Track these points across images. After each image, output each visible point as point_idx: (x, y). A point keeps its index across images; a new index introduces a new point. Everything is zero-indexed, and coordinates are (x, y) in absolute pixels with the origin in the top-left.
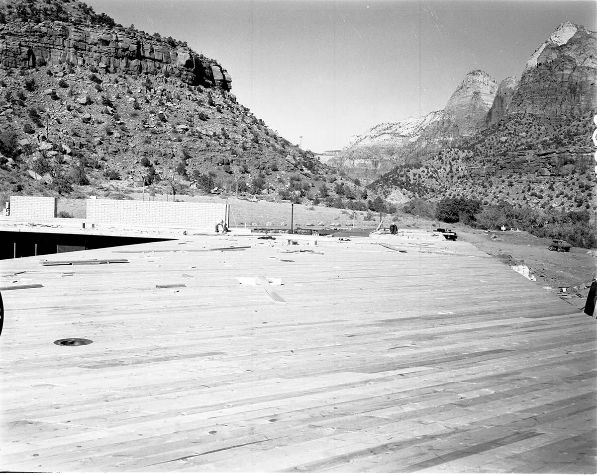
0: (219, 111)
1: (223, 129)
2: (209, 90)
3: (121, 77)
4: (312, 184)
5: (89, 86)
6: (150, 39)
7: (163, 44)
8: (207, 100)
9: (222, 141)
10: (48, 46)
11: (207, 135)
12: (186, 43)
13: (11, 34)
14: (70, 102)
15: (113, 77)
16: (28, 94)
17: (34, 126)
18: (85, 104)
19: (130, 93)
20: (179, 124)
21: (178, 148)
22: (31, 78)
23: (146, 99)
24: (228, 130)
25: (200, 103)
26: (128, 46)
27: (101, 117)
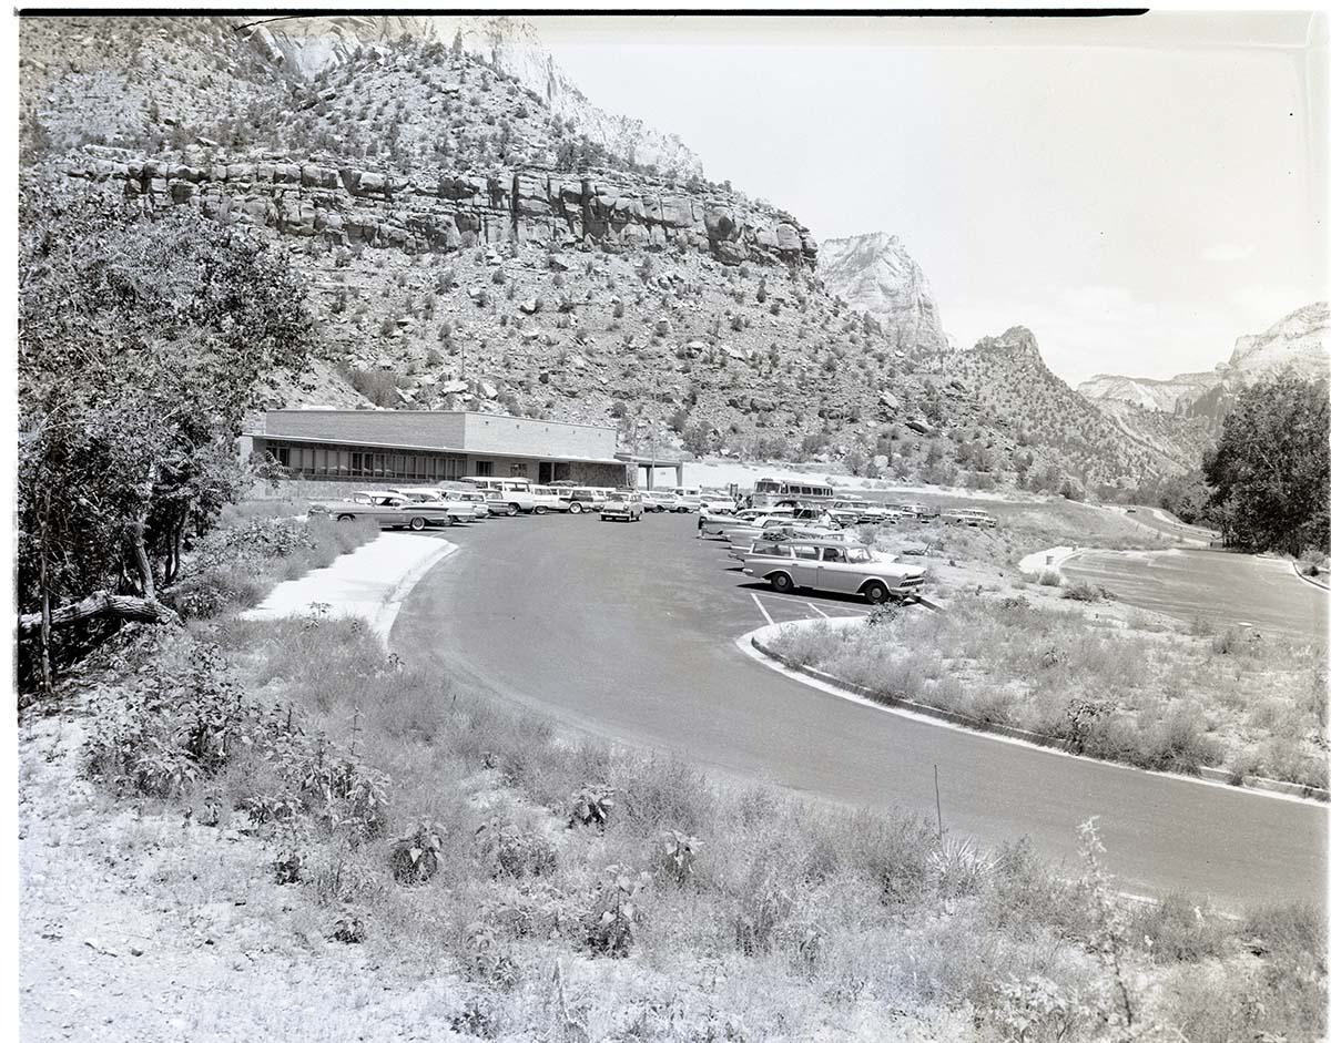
0: (775, 311)
1: (773, 347)
2: (765, 270)
5: (546, 277)
6: (656, 185)
7: (679, 190)
8: (756, 291)
9: (765, 369)
10: (483, 210)
11: (740, 359)
12: (727, 186)
13: (419, 193)
14: (508, 308)
15: (587, 258)
16: (440, 300)
17: (444, 353)
18: (529, 313)
19: (611, 287)
20: (690, 341)
22: (449, 269)
24: (784, 348)
25: (739, 298)
26: (614, 200)
27: (554, 334)
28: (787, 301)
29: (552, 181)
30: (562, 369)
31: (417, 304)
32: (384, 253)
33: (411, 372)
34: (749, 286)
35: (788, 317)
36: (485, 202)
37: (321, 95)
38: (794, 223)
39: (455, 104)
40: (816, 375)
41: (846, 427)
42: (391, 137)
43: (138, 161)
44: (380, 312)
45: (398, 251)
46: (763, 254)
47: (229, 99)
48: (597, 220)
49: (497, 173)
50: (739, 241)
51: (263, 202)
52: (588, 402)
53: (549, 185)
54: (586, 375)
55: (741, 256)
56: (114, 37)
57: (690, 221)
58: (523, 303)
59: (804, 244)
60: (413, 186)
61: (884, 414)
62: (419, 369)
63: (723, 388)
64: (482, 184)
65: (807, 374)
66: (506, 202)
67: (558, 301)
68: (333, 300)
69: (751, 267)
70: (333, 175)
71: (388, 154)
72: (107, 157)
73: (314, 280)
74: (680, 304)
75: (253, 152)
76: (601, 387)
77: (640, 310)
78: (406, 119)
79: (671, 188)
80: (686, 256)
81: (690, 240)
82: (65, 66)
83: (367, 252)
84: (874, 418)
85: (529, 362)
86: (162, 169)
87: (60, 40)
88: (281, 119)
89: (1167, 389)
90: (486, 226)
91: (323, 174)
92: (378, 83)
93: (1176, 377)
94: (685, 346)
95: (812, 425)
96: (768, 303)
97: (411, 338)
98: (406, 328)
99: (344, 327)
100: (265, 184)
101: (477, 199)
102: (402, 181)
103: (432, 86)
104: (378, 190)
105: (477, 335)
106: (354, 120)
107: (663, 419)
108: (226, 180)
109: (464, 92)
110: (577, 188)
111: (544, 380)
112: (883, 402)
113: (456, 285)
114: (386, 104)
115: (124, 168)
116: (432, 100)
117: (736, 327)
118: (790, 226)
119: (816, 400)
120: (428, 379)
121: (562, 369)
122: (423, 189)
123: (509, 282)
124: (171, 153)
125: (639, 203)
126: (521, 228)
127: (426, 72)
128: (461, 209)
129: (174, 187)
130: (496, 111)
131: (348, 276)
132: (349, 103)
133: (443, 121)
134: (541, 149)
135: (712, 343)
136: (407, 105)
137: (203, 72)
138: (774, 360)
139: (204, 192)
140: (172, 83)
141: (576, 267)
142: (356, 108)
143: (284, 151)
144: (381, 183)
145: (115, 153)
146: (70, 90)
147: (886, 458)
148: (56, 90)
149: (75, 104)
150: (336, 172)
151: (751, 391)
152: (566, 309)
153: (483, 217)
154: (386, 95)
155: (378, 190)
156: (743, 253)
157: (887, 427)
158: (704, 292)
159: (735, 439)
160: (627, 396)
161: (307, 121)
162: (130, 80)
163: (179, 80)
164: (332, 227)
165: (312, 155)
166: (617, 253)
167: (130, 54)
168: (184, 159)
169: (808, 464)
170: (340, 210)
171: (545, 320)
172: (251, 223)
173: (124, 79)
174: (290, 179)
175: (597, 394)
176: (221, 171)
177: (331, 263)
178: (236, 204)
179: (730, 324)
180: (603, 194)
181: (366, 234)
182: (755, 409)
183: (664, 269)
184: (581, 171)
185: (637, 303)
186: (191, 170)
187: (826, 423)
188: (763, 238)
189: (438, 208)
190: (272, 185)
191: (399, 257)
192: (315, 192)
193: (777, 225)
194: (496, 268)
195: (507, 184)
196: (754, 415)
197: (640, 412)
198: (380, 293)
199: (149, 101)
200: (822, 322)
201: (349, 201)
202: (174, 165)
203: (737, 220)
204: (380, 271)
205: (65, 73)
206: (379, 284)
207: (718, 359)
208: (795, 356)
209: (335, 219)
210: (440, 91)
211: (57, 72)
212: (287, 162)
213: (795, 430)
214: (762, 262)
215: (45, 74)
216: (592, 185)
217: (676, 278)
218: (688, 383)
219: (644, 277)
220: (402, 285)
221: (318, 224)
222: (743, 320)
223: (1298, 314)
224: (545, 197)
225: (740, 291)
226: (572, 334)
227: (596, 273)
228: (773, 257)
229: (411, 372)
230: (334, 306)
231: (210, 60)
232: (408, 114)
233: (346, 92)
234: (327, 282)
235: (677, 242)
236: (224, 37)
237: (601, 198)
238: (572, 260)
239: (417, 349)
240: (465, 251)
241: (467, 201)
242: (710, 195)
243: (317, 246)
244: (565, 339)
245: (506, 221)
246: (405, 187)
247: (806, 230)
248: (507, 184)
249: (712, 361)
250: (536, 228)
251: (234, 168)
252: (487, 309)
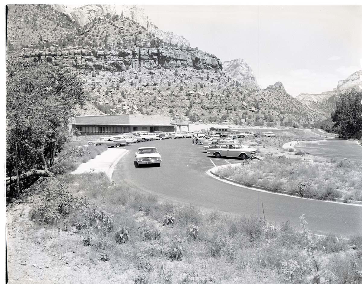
0: (212, 82)
1: (212, 91)
2: (209, 71)
3: (163, 70)
4: (254, 115)
5: (149, 76)
7: (184, 51)
9: (210, 98)
10: (131, 59)
12: (197, 49)
13: (113, 56)
14: (139, 85)
15: (160, 70)
17: (123, 99)
18: (145, 86)
19: (167, 78)
20: (189, 91)
21: (188, 103)
22: (122, 76)
23: (174, 80)
25: (202, 79)
27: (152, 91)
28: (215, 79)
30: (155, 101)
31: (115, 86)
32: (105, 72)
33: (114, 104)
34: (204, 75)
35: (216, 83)
36: (131, 57)
37: (86, 31)
38: (215, 58)
39: (122, 31)
40: (224, 98)
41: (233, 112)
42: (105, 41)
43: (37, 52)
44: (104, 88)
45: (109, 72)
46: (208, 66)
47: (61, 33)
48: (162, 60)
49: (134, 49)
50: (201, 63)
51: (72, 61)
52: (163, 109)
53: (148, 51)
54: (162, 102)
55: (202, 67)
56: (29, 19)
57: (187, 59)
58: (143, 84)
59: (219, 63)
60: (112, 54)
61: (243, 108)
62: (116, 103)
63: (199, 103)
64: (130, 52)
65: (222, 98)
66: (137, 57)
68: (92, 86)
69: (205, 70)
70: (90, 52)
71: (104, 46)
72: (29, 51)
73: (86, 81)
74: (186, 81)
75: (69, 47)
76: (166, 105)
77: (175, 84)
78: (109, 36)
79: (182, 50)
80: (187, 68)
81: (188, 64)
82: (16, 27)
83: (100, 72)
84: (240, 109)
85: (146, 100)
86: (44, 53)
87: (14, 20)
88: (75, 38)
89: (320, 97)
90: (132, 63)
91: (87, 52)
92: (101, 26)
93: (322, 93)
94: (188, 93)
95: (224, 112)
96: (210, 80)
97: (113, 95)
98: (112, 92)
99: (95, 93)
100: (72, 56)
101: (129, 56)
102: (109, 53)
103: (116, 27)
104: (102, 56)
105: (131, 93)
106: (95, 37)
107: (183, 113)
108: (61, 55)
109: (124, 27)
110: (156, 52)
111: (150, 104)
112: (243, 105)
113: (125, 80)
114: (103, 32)
115: (34, 54)
116: (116, 30)
117: (201, 87)
118: (214, 58)
119: (224, 105)
120: (119, 106)
121: (155, 101)
122: (115, 54)
123: (139, 78)
124: (46, 49)
125: (173, 55)
126: (142, 63)
127: (114, 23)
128: (125, 59)
129: (47, 58)
130: (133, 32)
131: (95, 79)
132: (93, 32)
133: (119, 36)
134: (146, 42)
135: (195, 91)
136: (109, 32)
137: (54, 27)
138: (212, 95)
139: (55, 59)
140: (45, 30)
141: (157, 73)
142: (95, 34)
143: (77, 47)
144: (103, 54)
145: (31, 50)
146: (18, 34)
147: (244, 120)
148: (14, 34)
149: (20, 37)
150: (91, 51)
151: (206, 104)
152: (155, 85)
153: (131, 61)
154: (104, 30)
155: (102, 56)
156: (202, 67)
157: (244, 111)
158: (192, 78)
159: (203, 117)
160: (173, 107)
161: (82, 38)
162: (34, 30)
163: (47, 29)
164: (90, 66)
165: (84, 47)
166: (168, 68)
167: (34, 23)
168: (50, 50)
169: (223, 123)
170: (92, 61)
171: (150, 88)
172: (68, 66)
173: (32, 30)
174: (78, 54)
175: (165, 107)
176: (60, 53)
177: (91, 76)
178: (64, 62)
179: (200, 86)
180: (163, 53)
181: (100, 68)
182: (208, 109)
183: (181, 72)
184: (157, 47)
185: (174, 82)
186: (52, 53)
187: (227, 111)
188: (207, 62)
189: (119, 59)
190: (74, 56)
191: (109, 73)
192: (85, 57)
193: (211, 58)
194: (135, 75)
195: (137, 52)
196: (208, 110)
197: (177, 111)
198: (104, 83)
199: (39, 35)
200: (225, 84)
201: (95, 59)
202: (47, 52)
203: (200, 58)
204: (104, 77)
205: (16, 29)
206: (104, 81)
207: (197, 96)
208: (218, 94)
209: (91, 64)
210: (118, 28)
211: (14, 29)
212: (77, 49)
213: (219, 113)
214: (207, 68)
215: (11, 30)
216: (160, 50)
217: (184, 74)
218: (189, 103)
219: (176, 75)
220: (110, 81)
221: (87, 66)
222: (203, 85)
223: (355, 74)
224: (148, 55)
225: (202, 77)
226: (157, 91)
227: (163, 74)
228: (210, 67)
229: (114, 104)
230: (92, 88)
231: (55, 23)
232: (109, 35)
233: (92, 30)
234: (90, 81)
235: (184, 65)
236: (59, 17)
237: (163, 54)
238: (156, 71)
239: (115, 98)
240: (127, 71)
242: (192, 51)
243: (87, 71)
244: (155, 93)
245: (137, 62)
246: (109, 54)
247: (219, 59)
248: (137, 52)
249: (195, 96)
250: (146, 63)
251: (63, 52)
252: (134, 86)
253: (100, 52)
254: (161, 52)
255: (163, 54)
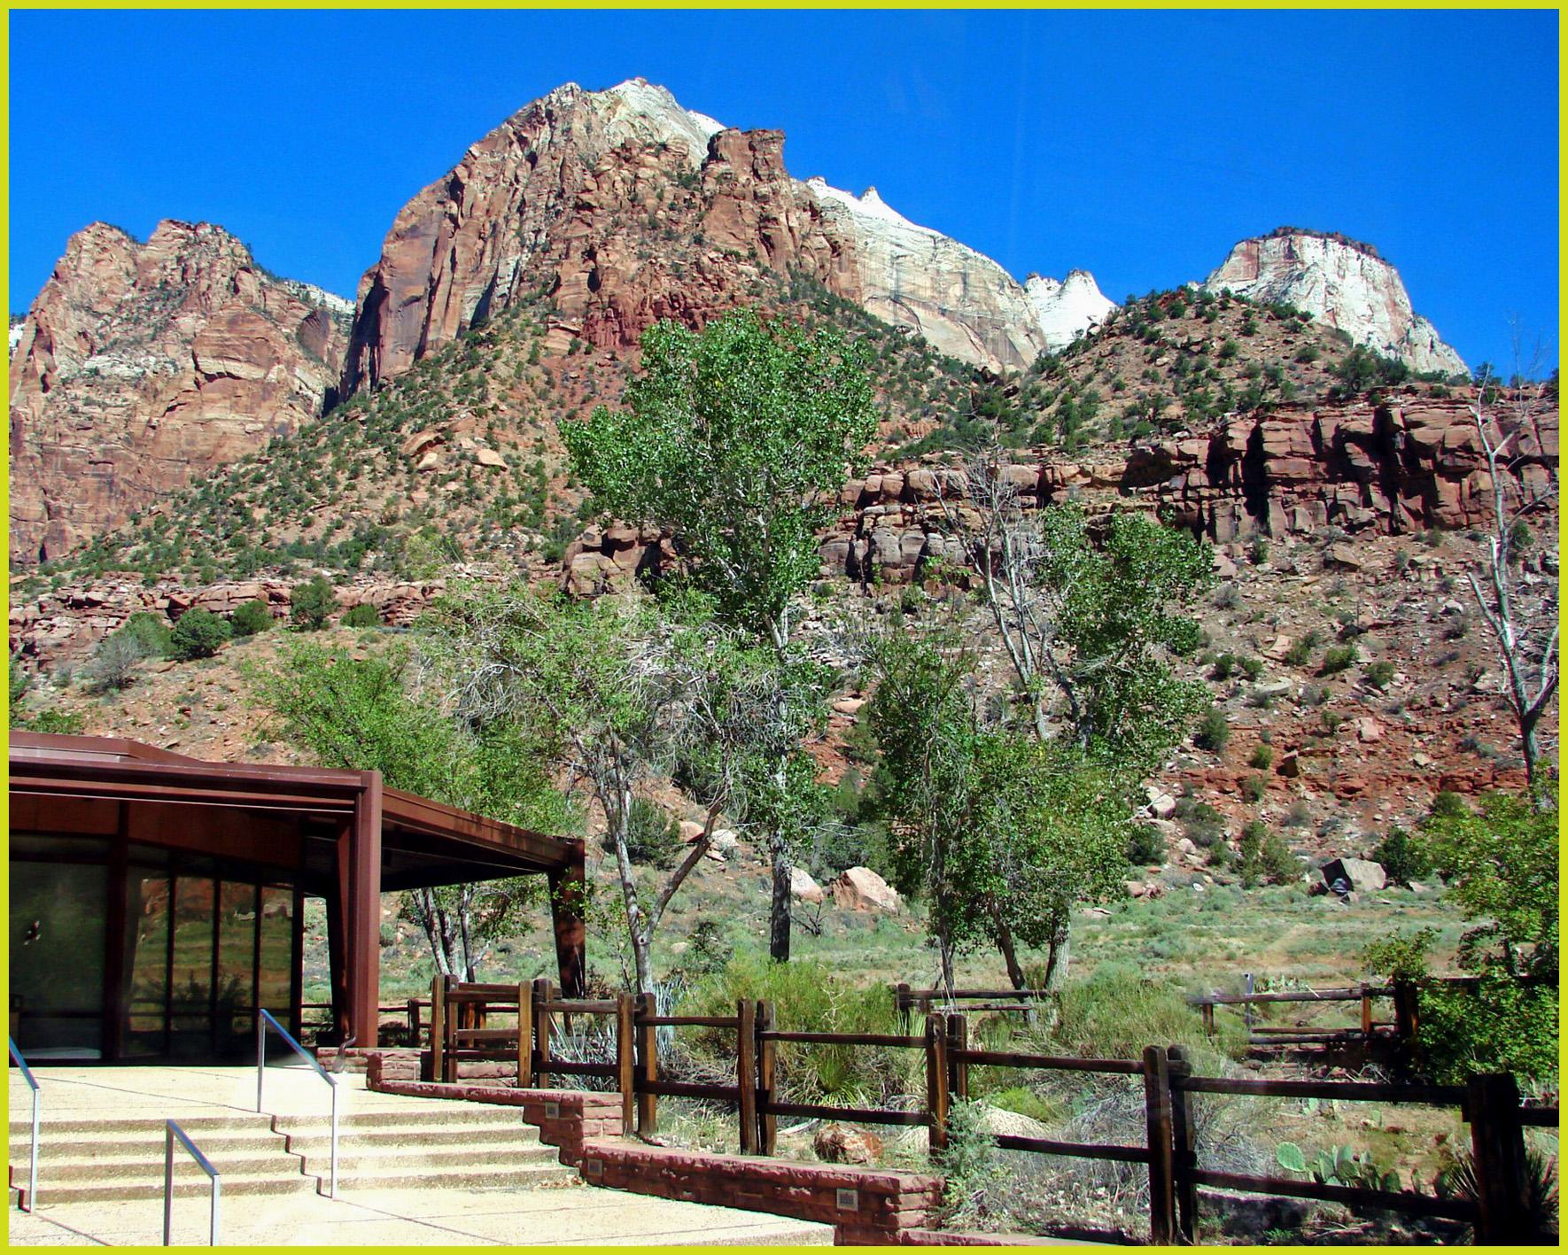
29: (1322, 422)
30: (1329, 743)
64: (1198, 448)
67: (1336, 624)
110: (1365, 425)
128: (1167, 498)
153: (1205, 504)
166: (1457, 527)
174: (882, 496)
180: (1418, 424)
224: (1312, 452)
238: (1373, 554)
241: (1178, 482)
248: (1239, 438)
253: (1018, 472)
254: (1398, 421)
255: (1418, 434)
